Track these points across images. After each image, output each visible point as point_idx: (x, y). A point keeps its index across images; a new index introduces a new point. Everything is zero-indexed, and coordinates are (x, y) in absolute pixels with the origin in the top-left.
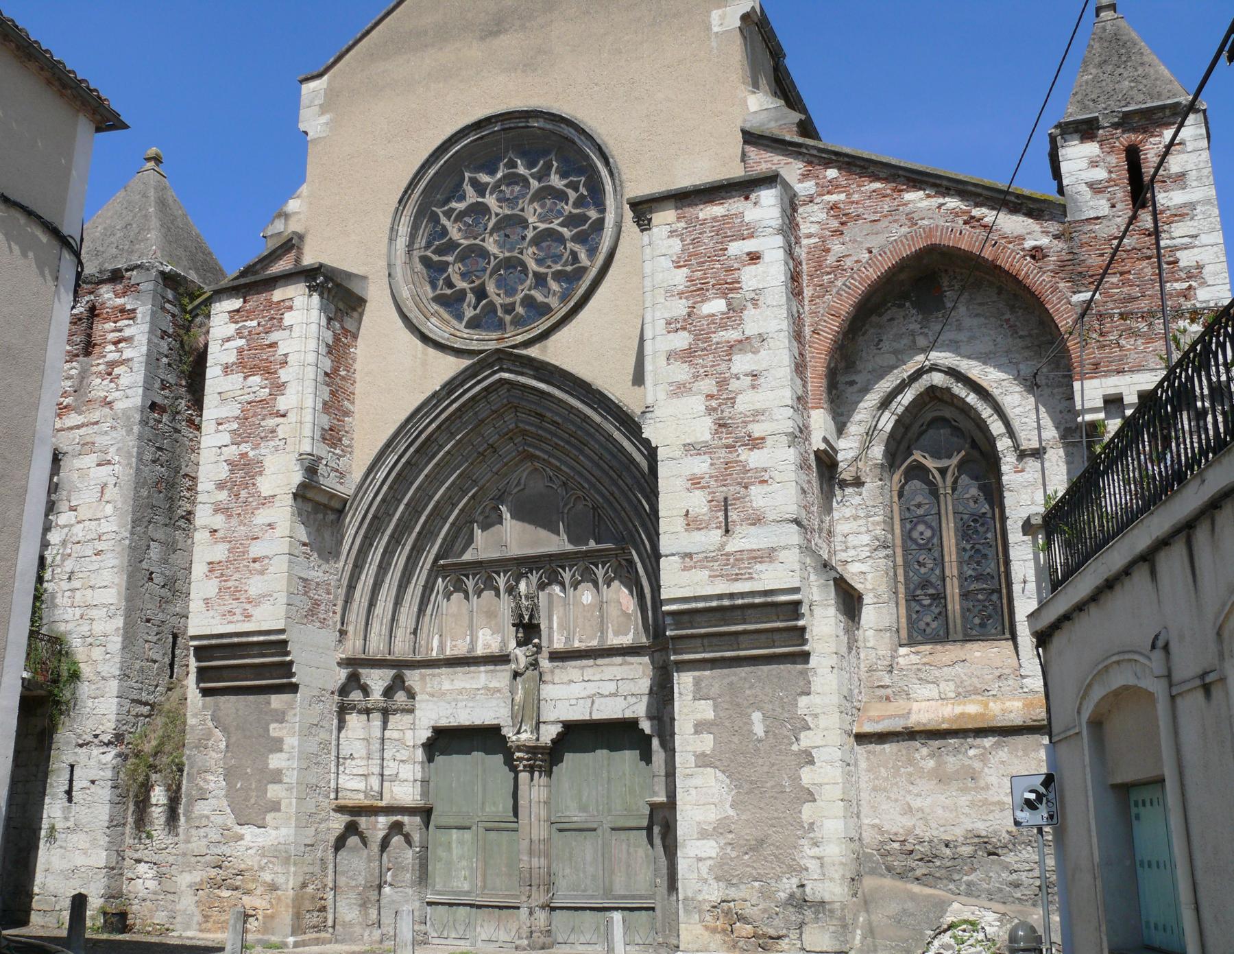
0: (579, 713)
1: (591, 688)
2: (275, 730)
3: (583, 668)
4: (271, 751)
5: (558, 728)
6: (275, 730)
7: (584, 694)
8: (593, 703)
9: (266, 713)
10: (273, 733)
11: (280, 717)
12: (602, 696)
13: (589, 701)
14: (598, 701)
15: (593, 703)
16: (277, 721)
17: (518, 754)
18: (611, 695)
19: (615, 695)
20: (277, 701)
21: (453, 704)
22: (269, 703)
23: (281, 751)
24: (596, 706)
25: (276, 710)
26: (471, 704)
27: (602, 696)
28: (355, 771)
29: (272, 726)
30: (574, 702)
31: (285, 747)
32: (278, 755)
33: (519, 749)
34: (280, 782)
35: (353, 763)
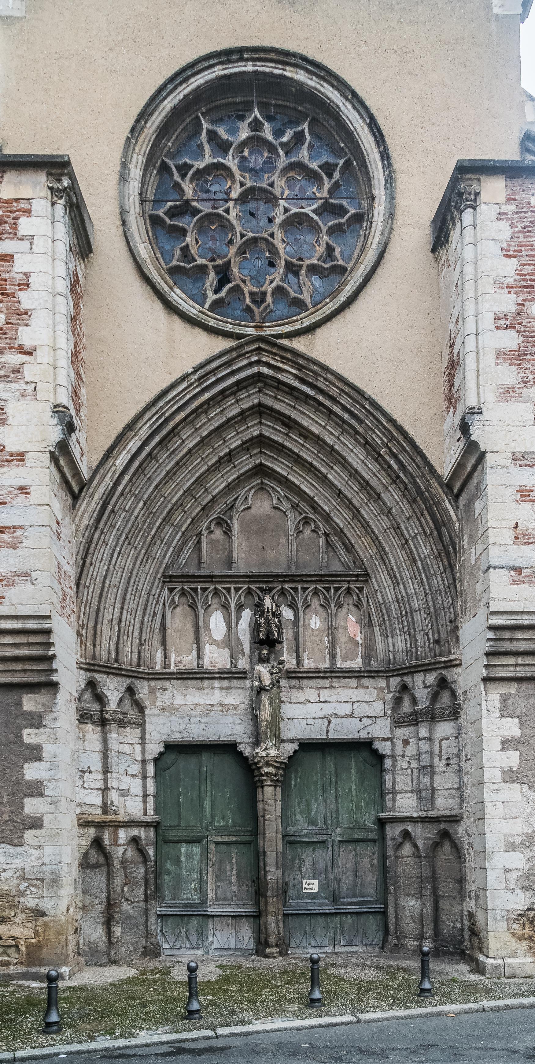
0: (316, 732)
1: (328, 709)
2: (30, 736)
3: (319, 689)
4: (27, 760)
5: (296, 746)
6: (30, 736)
7: (321, 714)
8: (329, 723)
9: (17, 717)
10: (27, 740)
11: (36, 721)
12: (338, 717)
13: (326, 721)
14: (334, 722)
15: (329, 723)
16: (32, 726)
17: (266, 770)
18: (346, 716)
19: (352, 716)
20: (30, 703)
21: (187, 719)
22: (20, 704)
23: (40, 759)
24: (331, 727)
25: (30, 713)
26: (204, 720)
27: (338, 717)
28: (93, 785)
29: (26, 732)
30: (311, 721)
31: (44, 755)
32: (36, 764)
33: (268, 764)
34: (41, 795)
35: (92, 776)
